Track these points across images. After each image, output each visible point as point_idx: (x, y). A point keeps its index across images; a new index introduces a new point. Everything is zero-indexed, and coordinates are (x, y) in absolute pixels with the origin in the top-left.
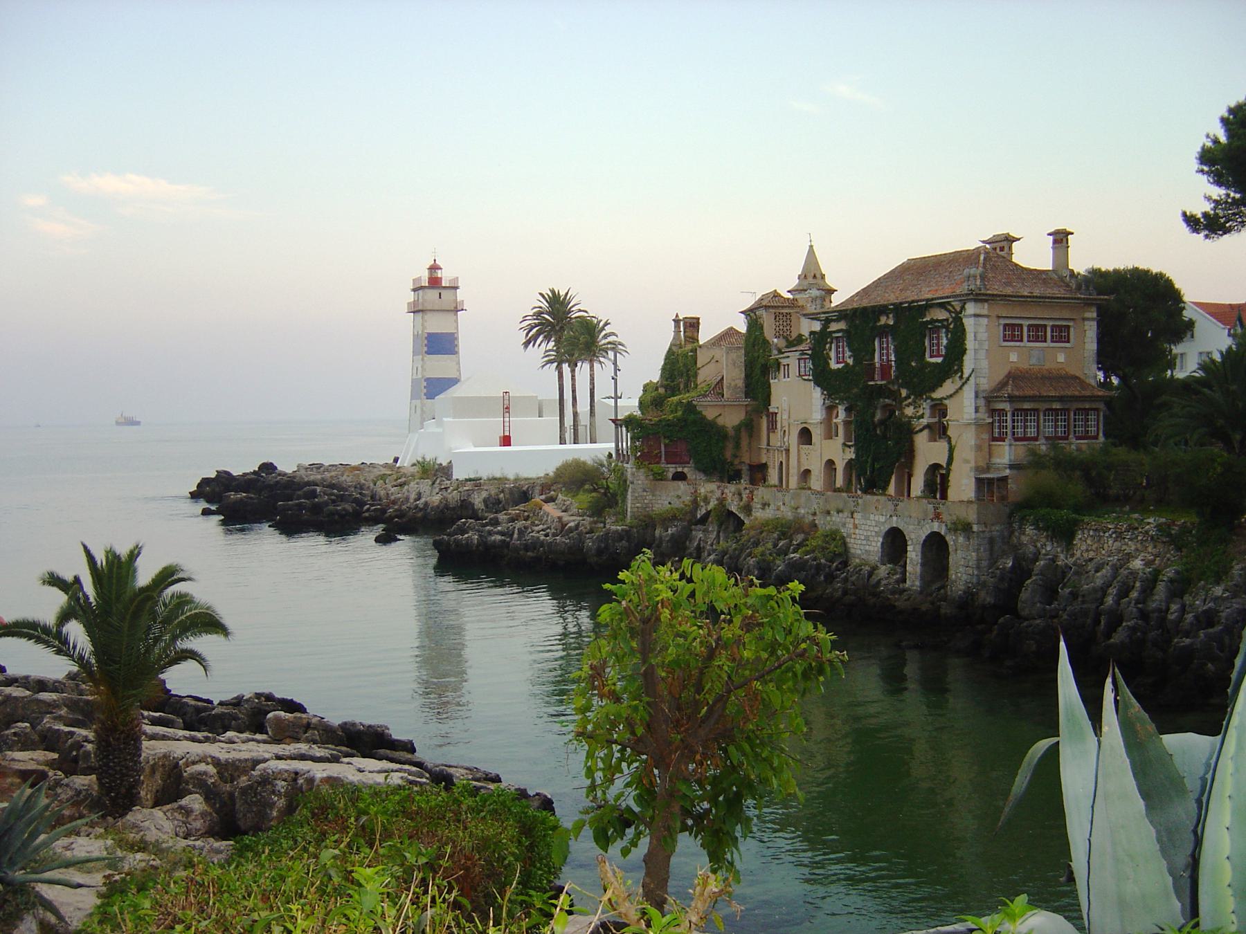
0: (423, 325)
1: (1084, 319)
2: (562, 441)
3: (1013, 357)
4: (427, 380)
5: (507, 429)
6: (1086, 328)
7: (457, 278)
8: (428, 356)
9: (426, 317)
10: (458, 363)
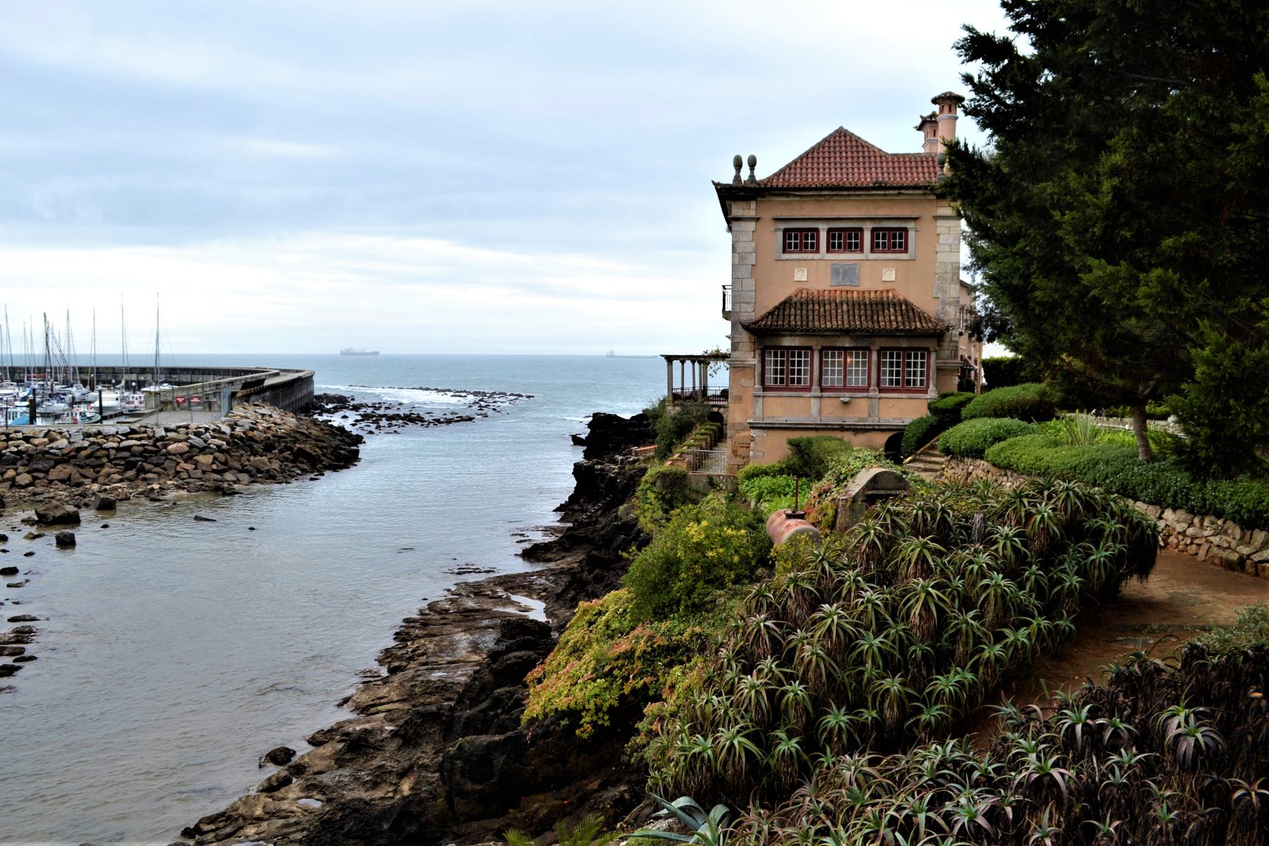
1: (937, 218)
3: (801, 275)
6: (939, 231)
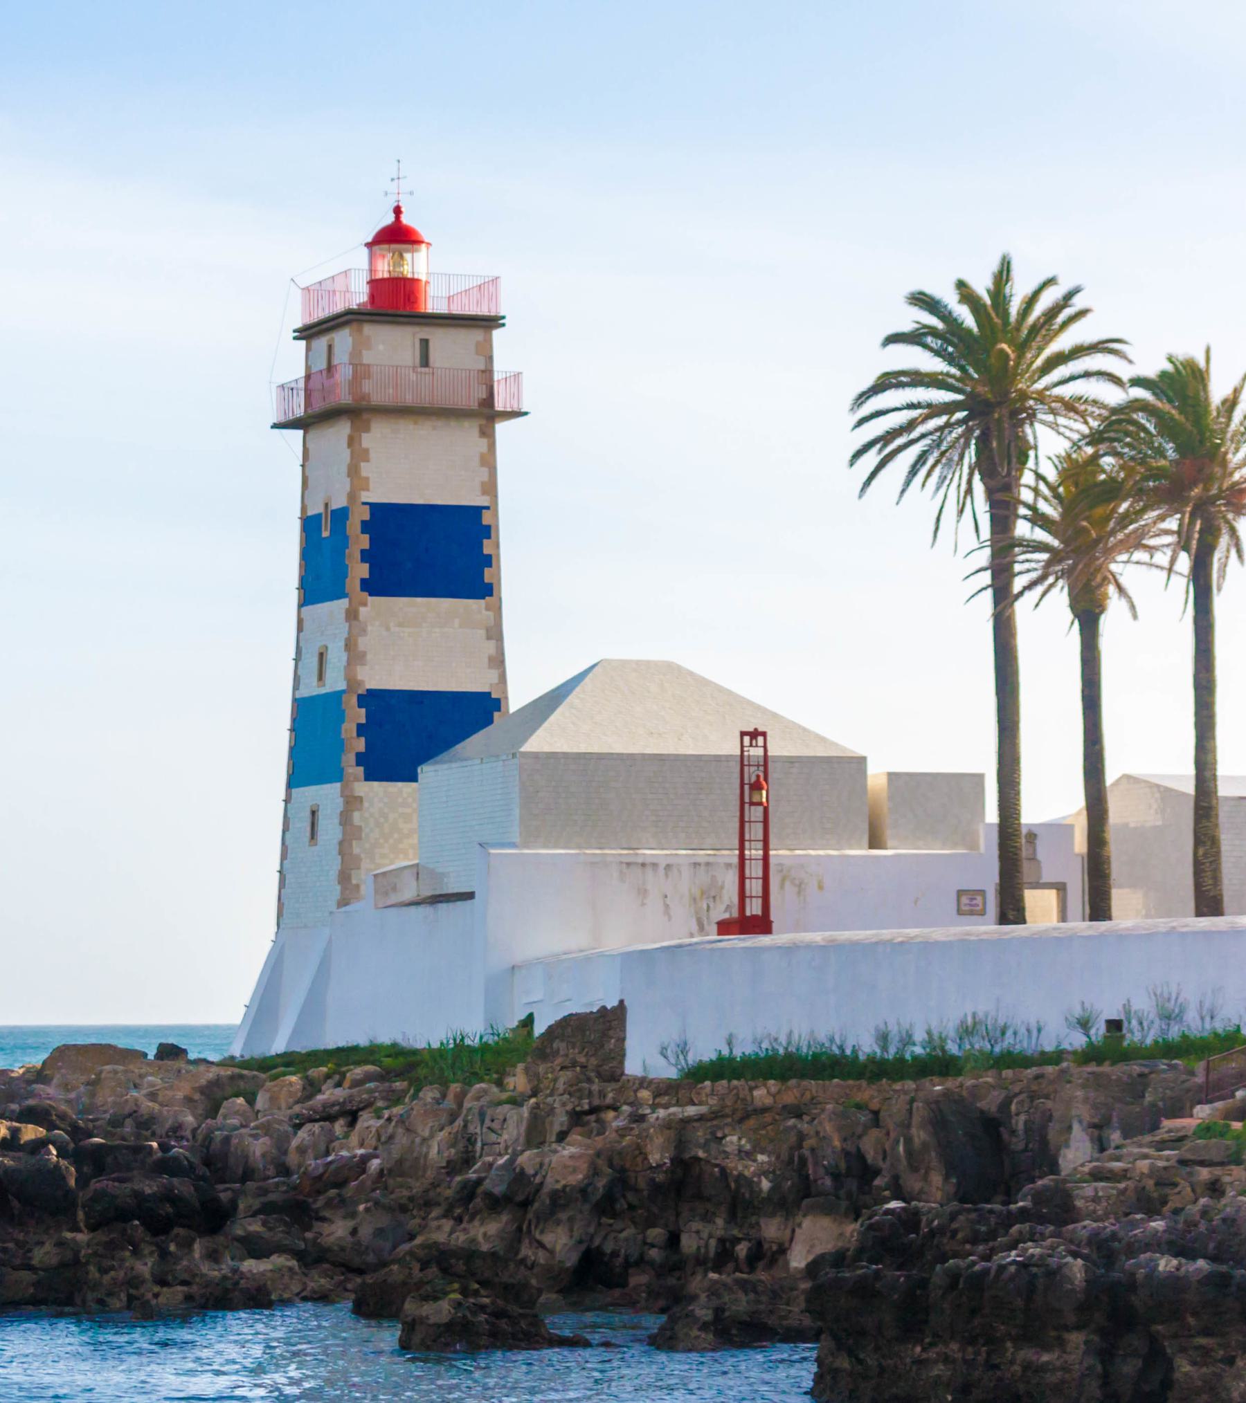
0: (353, 471)
2: (1063, 917)
4: (375, 700)
5: (754, 887)
7: (495, 280)
8: (370, 599)
9: (367, 440)
10: (495, 633)
